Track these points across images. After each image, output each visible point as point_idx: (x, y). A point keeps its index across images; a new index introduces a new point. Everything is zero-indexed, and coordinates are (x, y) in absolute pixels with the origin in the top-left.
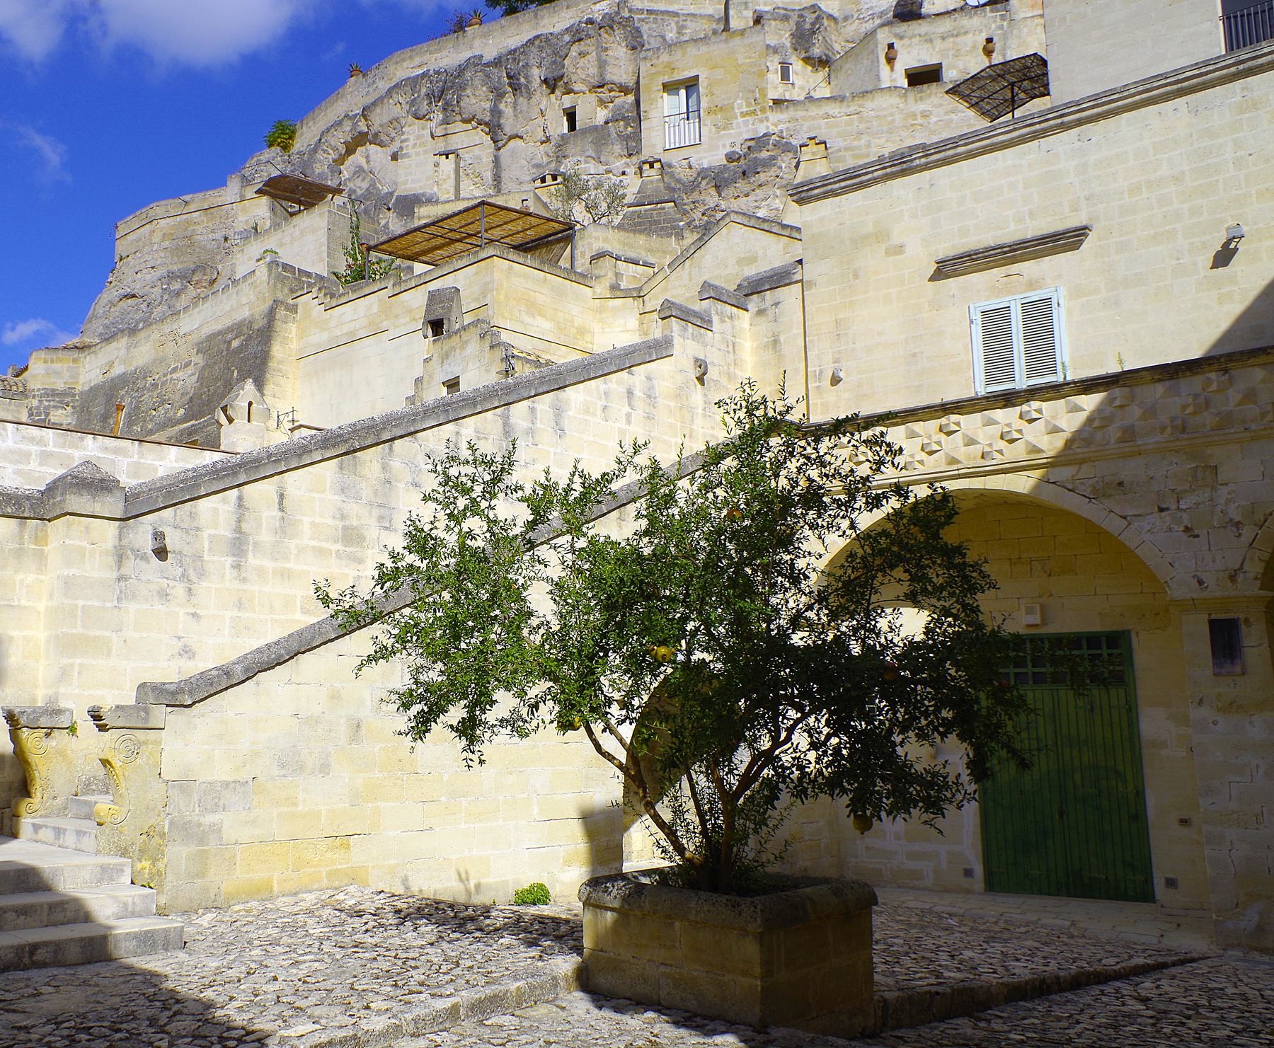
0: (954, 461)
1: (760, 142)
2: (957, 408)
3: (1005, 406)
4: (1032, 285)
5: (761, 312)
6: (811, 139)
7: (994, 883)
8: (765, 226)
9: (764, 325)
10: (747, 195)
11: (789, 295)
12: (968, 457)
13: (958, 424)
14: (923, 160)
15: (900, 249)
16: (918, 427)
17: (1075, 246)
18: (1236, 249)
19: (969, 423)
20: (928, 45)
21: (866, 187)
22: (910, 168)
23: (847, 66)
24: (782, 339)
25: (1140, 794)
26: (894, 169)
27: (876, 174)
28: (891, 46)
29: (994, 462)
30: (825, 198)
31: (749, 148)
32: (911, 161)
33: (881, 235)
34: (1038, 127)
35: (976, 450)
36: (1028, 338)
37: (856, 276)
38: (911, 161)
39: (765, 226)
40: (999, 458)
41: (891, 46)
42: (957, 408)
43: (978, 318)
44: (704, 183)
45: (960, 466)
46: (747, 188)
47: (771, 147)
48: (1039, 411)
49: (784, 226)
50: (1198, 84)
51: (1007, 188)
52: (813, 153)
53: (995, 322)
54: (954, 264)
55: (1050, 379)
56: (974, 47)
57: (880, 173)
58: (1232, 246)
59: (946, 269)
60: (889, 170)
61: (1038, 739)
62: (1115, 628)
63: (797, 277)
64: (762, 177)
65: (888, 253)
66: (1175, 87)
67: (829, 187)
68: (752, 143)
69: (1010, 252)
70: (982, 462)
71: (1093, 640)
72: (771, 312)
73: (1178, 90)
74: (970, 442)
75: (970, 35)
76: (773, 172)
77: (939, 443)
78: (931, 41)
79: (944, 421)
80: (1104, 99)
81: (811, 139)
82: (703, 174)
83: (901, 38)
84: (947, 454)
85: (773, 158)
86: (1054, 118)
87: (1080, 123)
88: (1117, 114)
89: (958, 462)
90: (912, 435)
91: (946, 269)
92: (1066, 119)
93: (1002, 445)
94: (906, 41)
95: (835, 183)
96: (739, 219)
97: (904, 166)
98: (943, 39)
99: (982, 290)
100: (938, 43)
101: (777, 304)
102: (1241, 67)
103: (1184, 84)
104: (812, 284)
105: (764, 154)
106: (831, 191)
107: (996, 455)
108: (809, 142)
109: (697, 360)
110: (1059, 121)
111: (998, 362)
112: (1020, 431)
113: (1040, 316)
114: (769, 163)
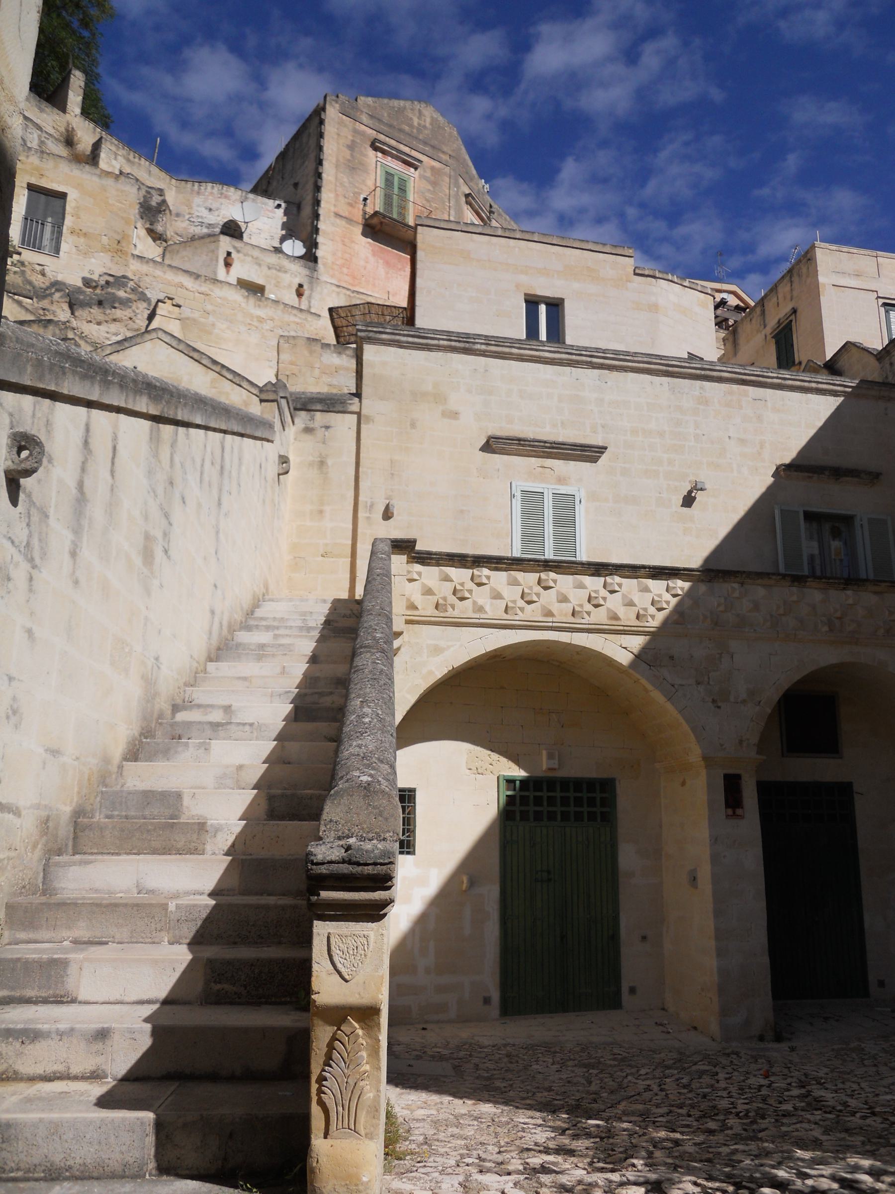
0: (549, 614)
1: (120, 281)
2: (556, 567)
3: (593, 575)
4: (561, 480)
5: (308, 430)
6: (170, 298)
7: (511, 1006)
8: (196, 355)
9: (309, 442)
10: (99, 324)
11: (344, 423)
12: (562, 612)
13: (555, 581)
14: (483, 347)
15: (454, 415)
16: (520, 576)
17: (594, 460)
18: (695, 498)
19: (499, 579)
20: (257, 267)
21: (429, 350)
23: (184, 253)
24: (330, 462)
25: (616, 919)
27: (442, 342)
28: (229, 254)
29: (583, 621)
30: (389, 345)
31: (107, 282)
33: (439, 398)
34: (574, 357)
35: (568, 608)
36: (556, 523)
37: (413, 425)
39: (196, 355)
40: (521, 616)
41: (229, 254)
42: (556, 567)
43: (518, 495)
44: (57, 295)
45: (550, 619)
46: (101, 317)
47: (128, 290)
48: (620, 585)
49: (215, 362)
50: (678, 373)
51: (541, 397)
52: (169, 312)
53: (532, 502)
54: (505, 444)
55: (574, 559)
56: (290, 286)
57: (445, 343)
58: (693, 495)
59: (492, 445)
60: (453, 344)
61: (549, 872)
63: (355, 408)
64: (118, 313)
65: (444, 414)
66: (664, 368)
67: (398, 337)
68: (111, 279)
69: (549, 448)
70: (572, 620)
71: (591, 784)
72: (320, 433)
73: (667, 371)
74: (563, 599)
75: (288, 275)
76: (128, 313)
77: (538, 595)
78: (260, 265)
79: (543, 575)
80: (621, 357)
81: (170, 298)
82: (57, 285)
83: (238, 251)
84: (543, 607)
85: (129, 300)
87: (601, 367)
88: (626, 371)
89: (552, 615)
90: (515, 583)
91: (492, 445)
92: (595, 360)
93: (588, 607)
94: (241, 255)
95: (404, 335)
96: (167, 339)
97: (467, 345)
98: (269, 268)
99: (523, 472)
100: (265, 269)
101: (327, 427)
102: (703, 372)
103: (670, 369)
104: (369, 419)
105: (121, 294)
106: (398, 341)
107: (585, 615)
108: (166, 300)
109: (281, 457)
110: (589, 359)
111: (532, 536)
112: (604, 599)
113: (566, 507)
114: (125, 303)
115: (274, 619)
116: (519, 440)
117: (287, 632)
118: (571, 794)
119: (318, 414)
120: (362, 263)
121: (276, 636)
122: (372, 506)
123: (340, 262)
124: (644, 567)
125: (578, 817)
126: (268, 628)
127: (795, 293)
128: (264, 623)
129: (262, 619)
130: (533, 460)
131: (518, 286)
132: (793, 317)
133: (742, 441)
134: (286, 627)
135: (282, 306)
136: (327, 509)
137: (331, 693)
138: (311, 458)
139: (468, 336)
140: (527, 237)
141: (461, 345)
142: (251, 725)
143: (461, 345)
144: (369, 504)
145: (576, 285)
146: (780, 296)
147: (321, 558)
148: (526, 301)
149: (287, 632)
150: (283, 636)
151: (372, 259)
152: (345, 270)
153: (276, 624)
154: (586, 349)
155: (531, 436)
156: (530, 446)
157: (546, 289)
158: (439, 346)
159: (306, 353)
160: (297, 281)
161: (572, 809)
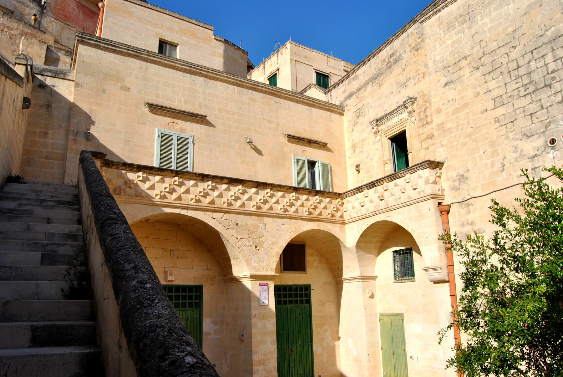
14: (146, 56)
15: (128, 89)
22: (139, 56)
24: (53, 106)
26: (132, 53)
32: (141, 54)
37: (104, 91)
38: (141, 54)
60: (130, 52)
62: (198, 284)
67: (99, 44)
71: (190, 288)
73: (237, 83)
86: (199, 69)
92: (203, 72)
95: (103, 43)
99: (163, 124)
106: (99, 46)
115: (18, 193)
116: (162, 107)
117: (26, 202)
118: (181, 294)
119: (48, 78)
120: (71, 10)
121: (20, 205)
122: (77, 133)
123: (58, 7)
124: (226, 178)
125: (184, 305)
126: (14, 199)
127: (279, 61)
128: (11, 195)
129: (9, 193)
130: (168, 118)
131: (156, 34)
132: (277, 72)
133: (270, 121)
134: (26, 199)
135: (23, 24)
136: (50, 132)
137: (65, 244)
138: (42, 102)
139: (138, 49)
140: (163, 11)
141: (135, 53)
142: (11, 267)
143: (135, 53)
144: (76, 132)
145: (185, 39)
146: (273, 61)
147: (44, 160)
148: (160, 41)
149: (26, 202)
150: (25, 205)
151: (77, 10)
152: (61, 12)
153: (18, 196)
154: (199, 66)
155: (168, 106)
156: (167, 111)
157: (168, 38)
158: (122, 52)
159: (38, 49)
160: (34, 12)
161: (181, 301)
